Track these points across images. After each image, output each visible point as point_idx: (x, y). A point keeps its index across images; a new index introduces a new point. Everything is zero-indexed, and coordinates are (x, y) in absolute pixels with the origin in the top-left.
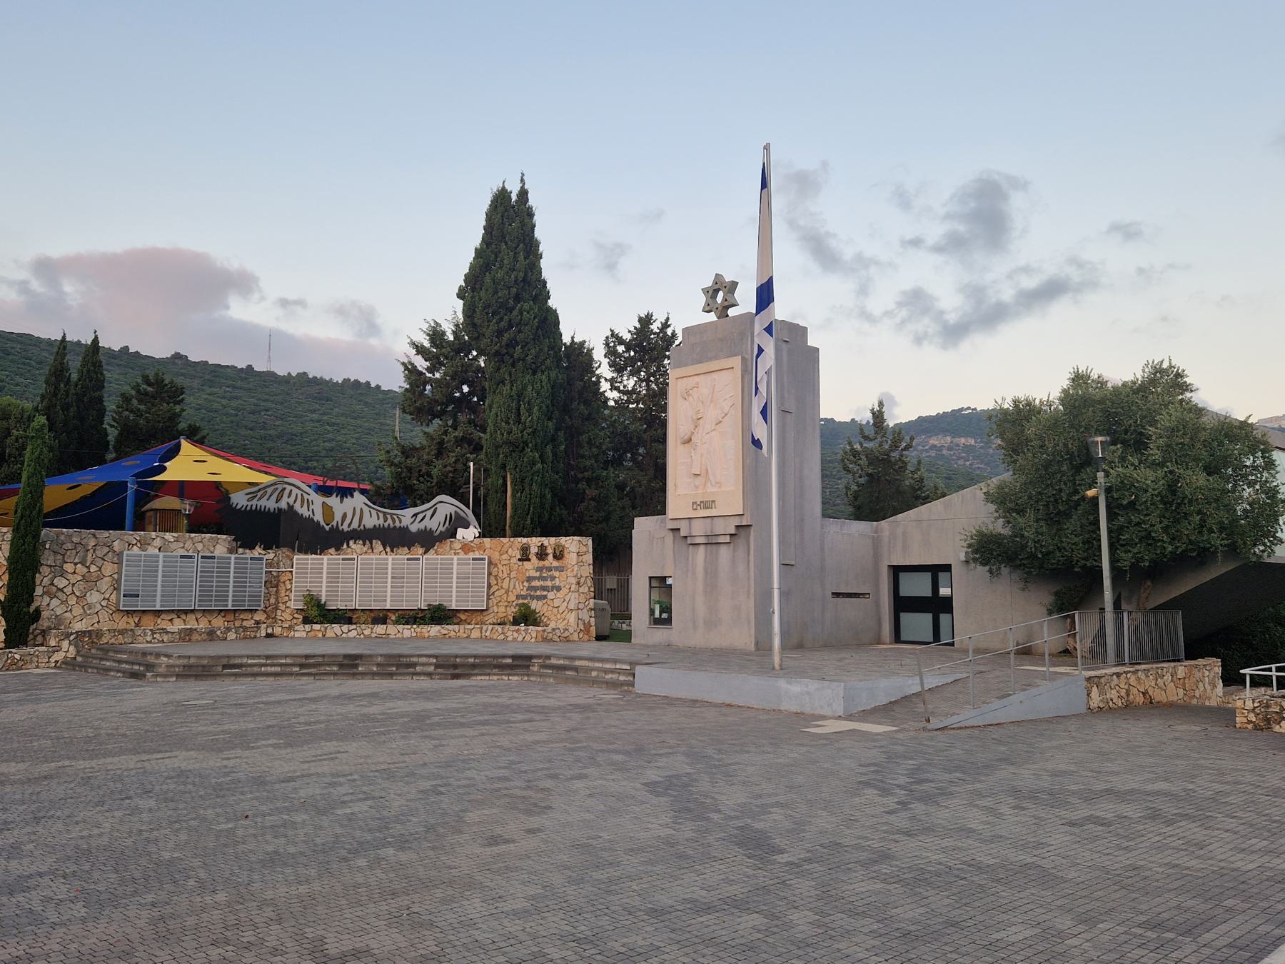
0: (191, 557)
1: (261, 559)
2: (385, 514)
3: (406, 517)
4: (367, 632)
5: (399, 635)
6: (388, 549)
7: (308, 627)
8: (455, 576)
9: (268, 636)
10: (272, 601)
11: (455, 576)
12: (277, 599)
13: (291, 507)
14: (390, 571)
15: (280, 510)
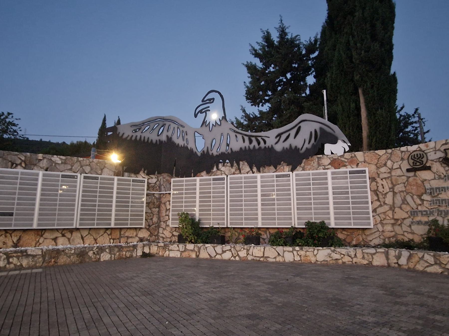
0: (73, 177)
1: (143, 182)
2: (250, 137)
3: (270, 137)
4: (243, 254)
5: (279, 259)
6: (255, 169)
7: (181, 246)
8: (330, 191)
9: (145, 255)
10: (155, 219)
11: (330, 191)
12: (159, 218)
13: (169, 139)
14: (259, 189)
15: (161, 142)
